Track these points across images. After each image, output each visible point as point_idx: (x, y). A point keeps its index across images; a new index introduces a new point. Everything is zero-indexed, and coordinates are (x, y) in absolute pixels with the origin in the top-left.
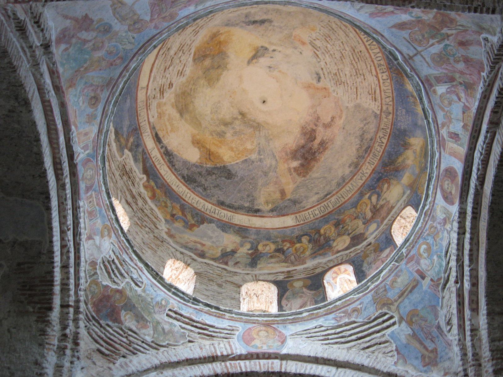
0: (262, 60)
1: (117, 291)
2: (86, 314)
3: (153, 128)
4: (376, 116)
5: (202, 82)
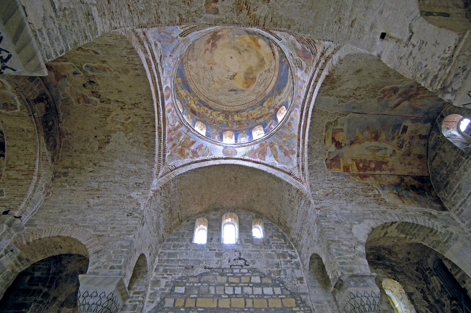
0: (232, 74)
3: (275, 58)
4: (189, 60)
5: (254, 69)
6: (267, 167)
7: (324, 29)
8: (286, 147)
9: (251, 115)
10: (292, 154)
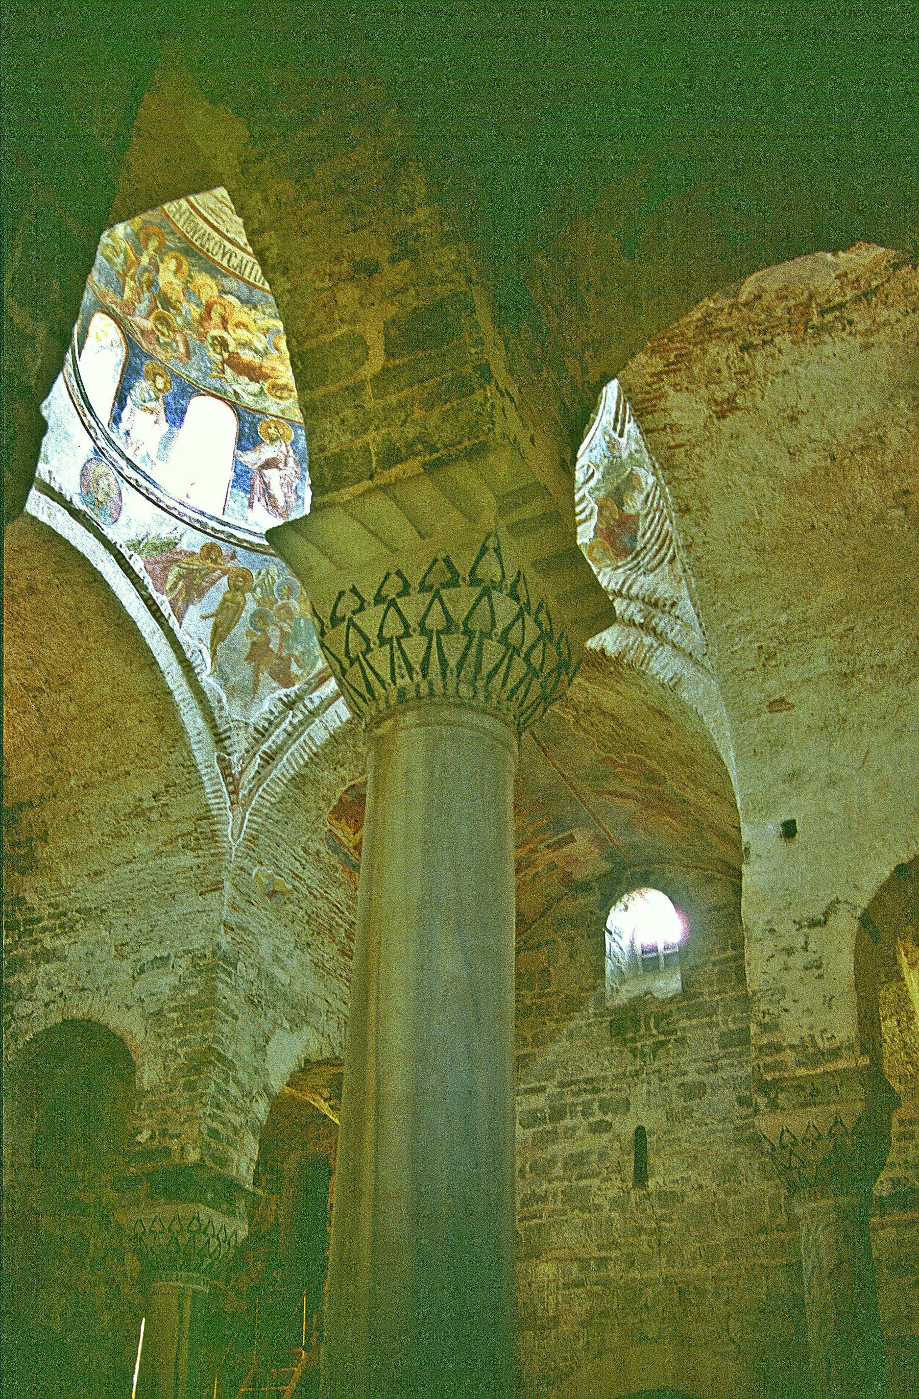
1: (600, 514)
2: (630, 569)
6: (172, 656)
7: (729, 622)
8: (274, 633)
9: (224, 322)
10: (274, 676)
